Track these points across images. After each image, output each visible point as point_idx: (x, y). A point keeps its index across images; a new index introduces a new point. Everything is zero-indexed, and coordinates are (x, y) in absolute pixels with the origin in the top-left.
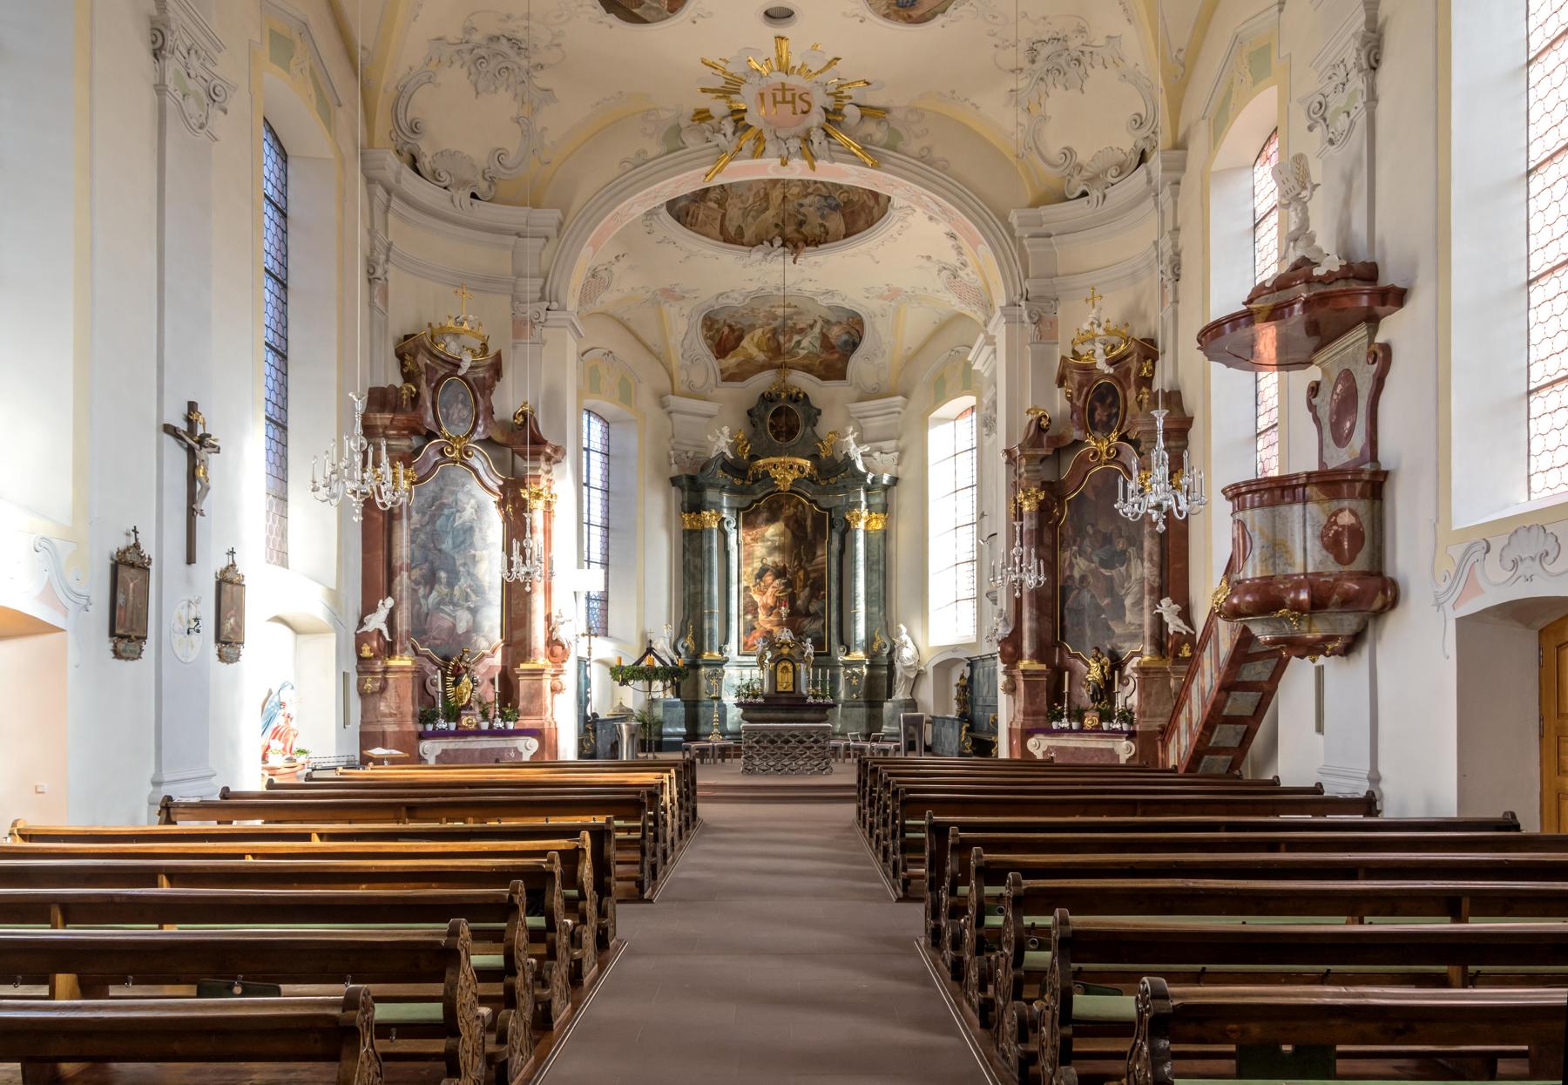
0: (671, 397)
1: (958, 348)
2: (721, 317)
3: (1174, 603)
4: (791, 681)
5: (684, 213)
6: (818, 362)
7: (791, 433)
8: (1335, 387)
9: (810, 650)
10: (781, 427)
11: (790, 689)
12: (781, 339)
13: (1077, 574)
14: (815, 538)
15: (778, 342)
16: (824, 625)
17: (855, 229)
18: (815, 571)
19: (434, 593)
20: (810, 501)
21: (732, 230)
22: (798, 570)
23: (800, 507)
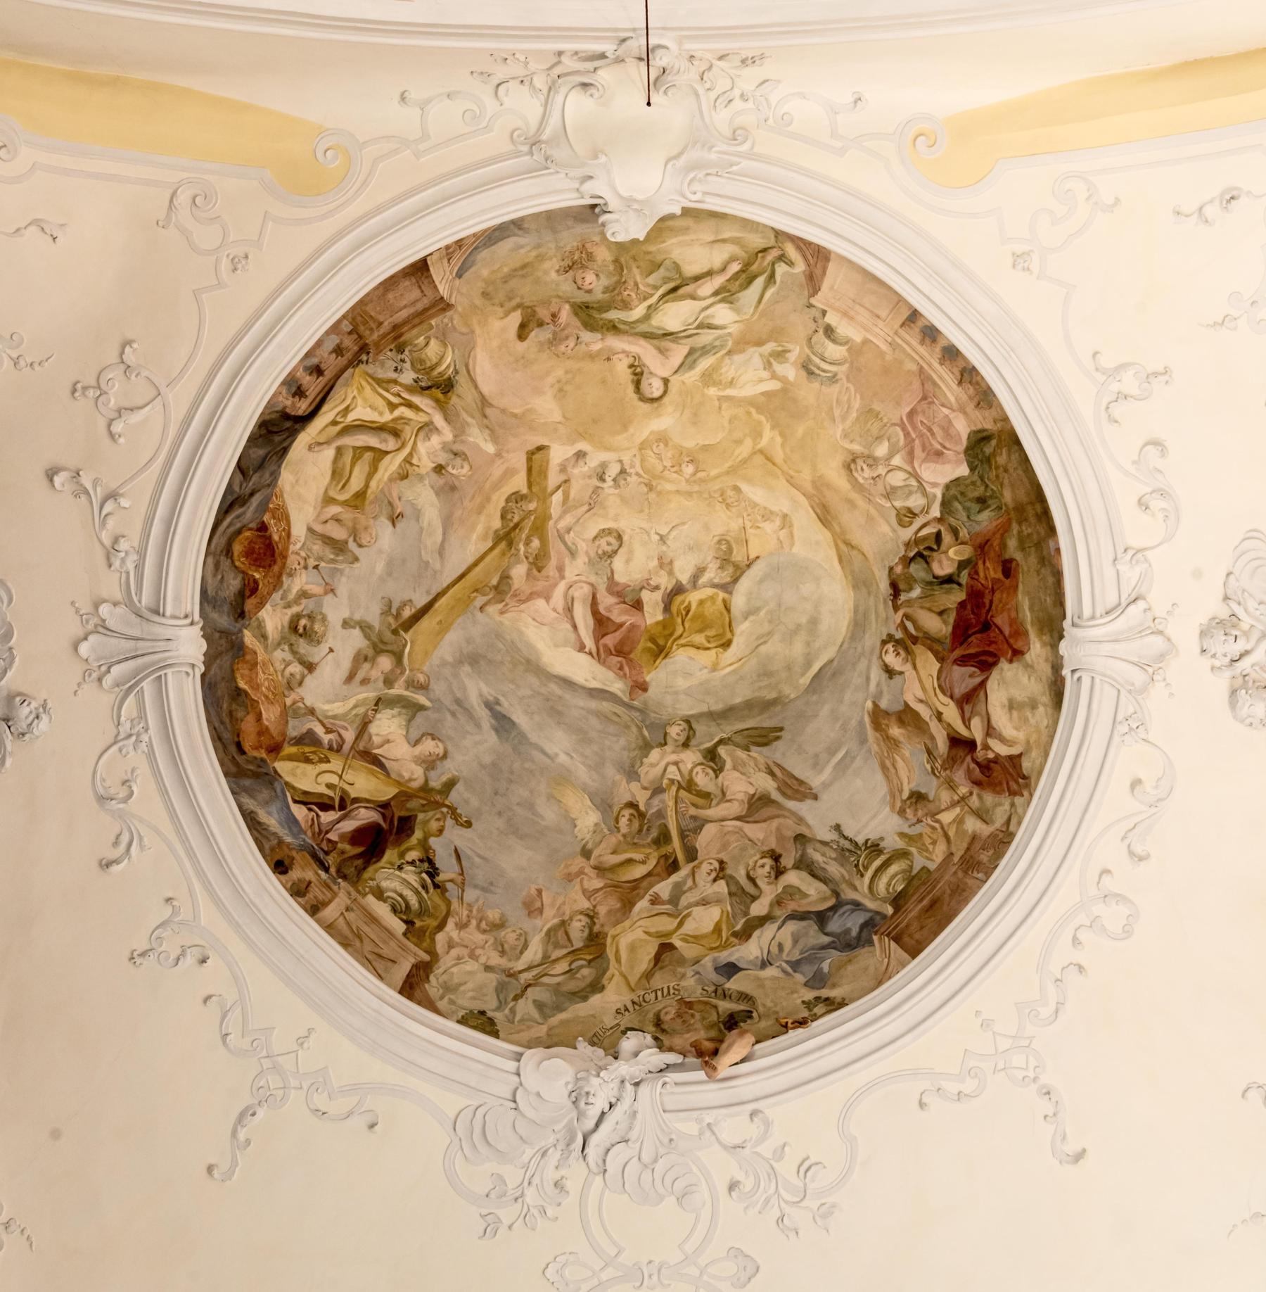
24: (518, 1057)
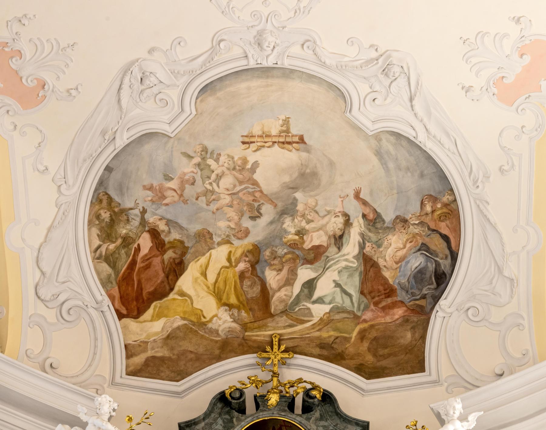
6: (355, 334)
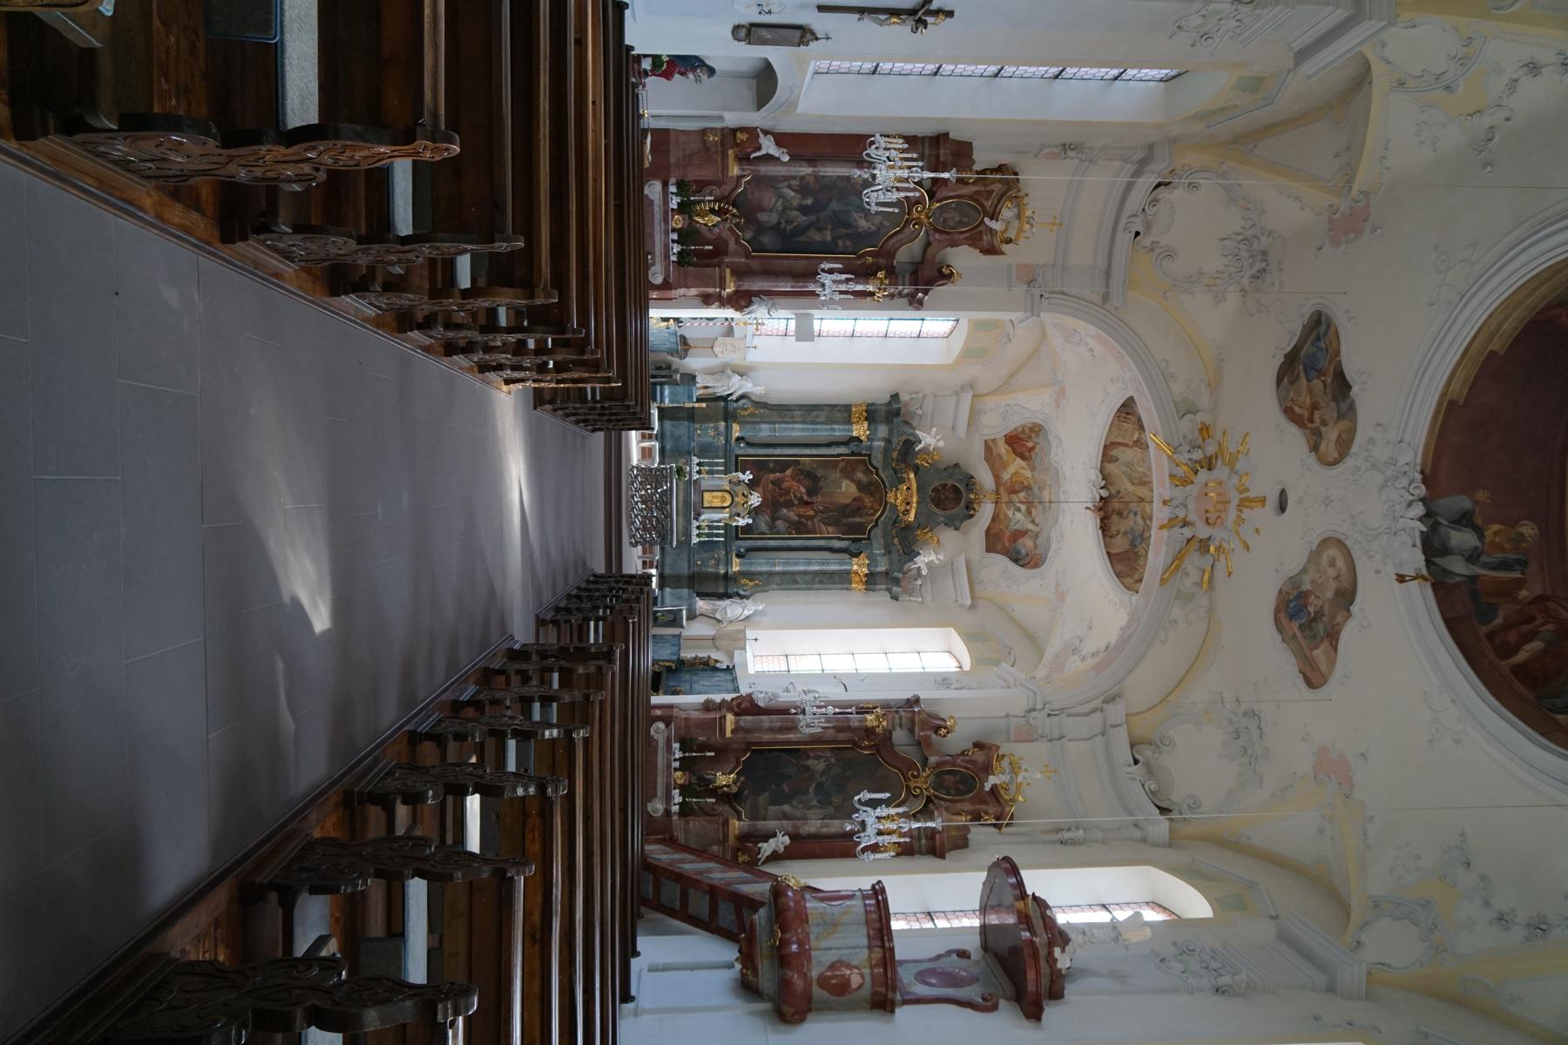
0: (972, 394)
1: (1012, 653)
2: (1041, 440)
3: (785, 847)
4: (714, 505)
5: (1128, 411)
6: (1001, 526)
7: (938, 502)
8: (965, 971)
9: (742, 522)
10: (944, 494)
11: (705, 505)
12: (1022, 495)
13: (810, 762)
14: (843, 525)
15: (1019, 492)
16: (764, 533)
17: (1114, 562)
18: (813, 524)
19: (792, 194)
20: (877, 520)
21: (1114, 453)
22: (814, 510)
23: (872, 511)
24: (1096, 469)
